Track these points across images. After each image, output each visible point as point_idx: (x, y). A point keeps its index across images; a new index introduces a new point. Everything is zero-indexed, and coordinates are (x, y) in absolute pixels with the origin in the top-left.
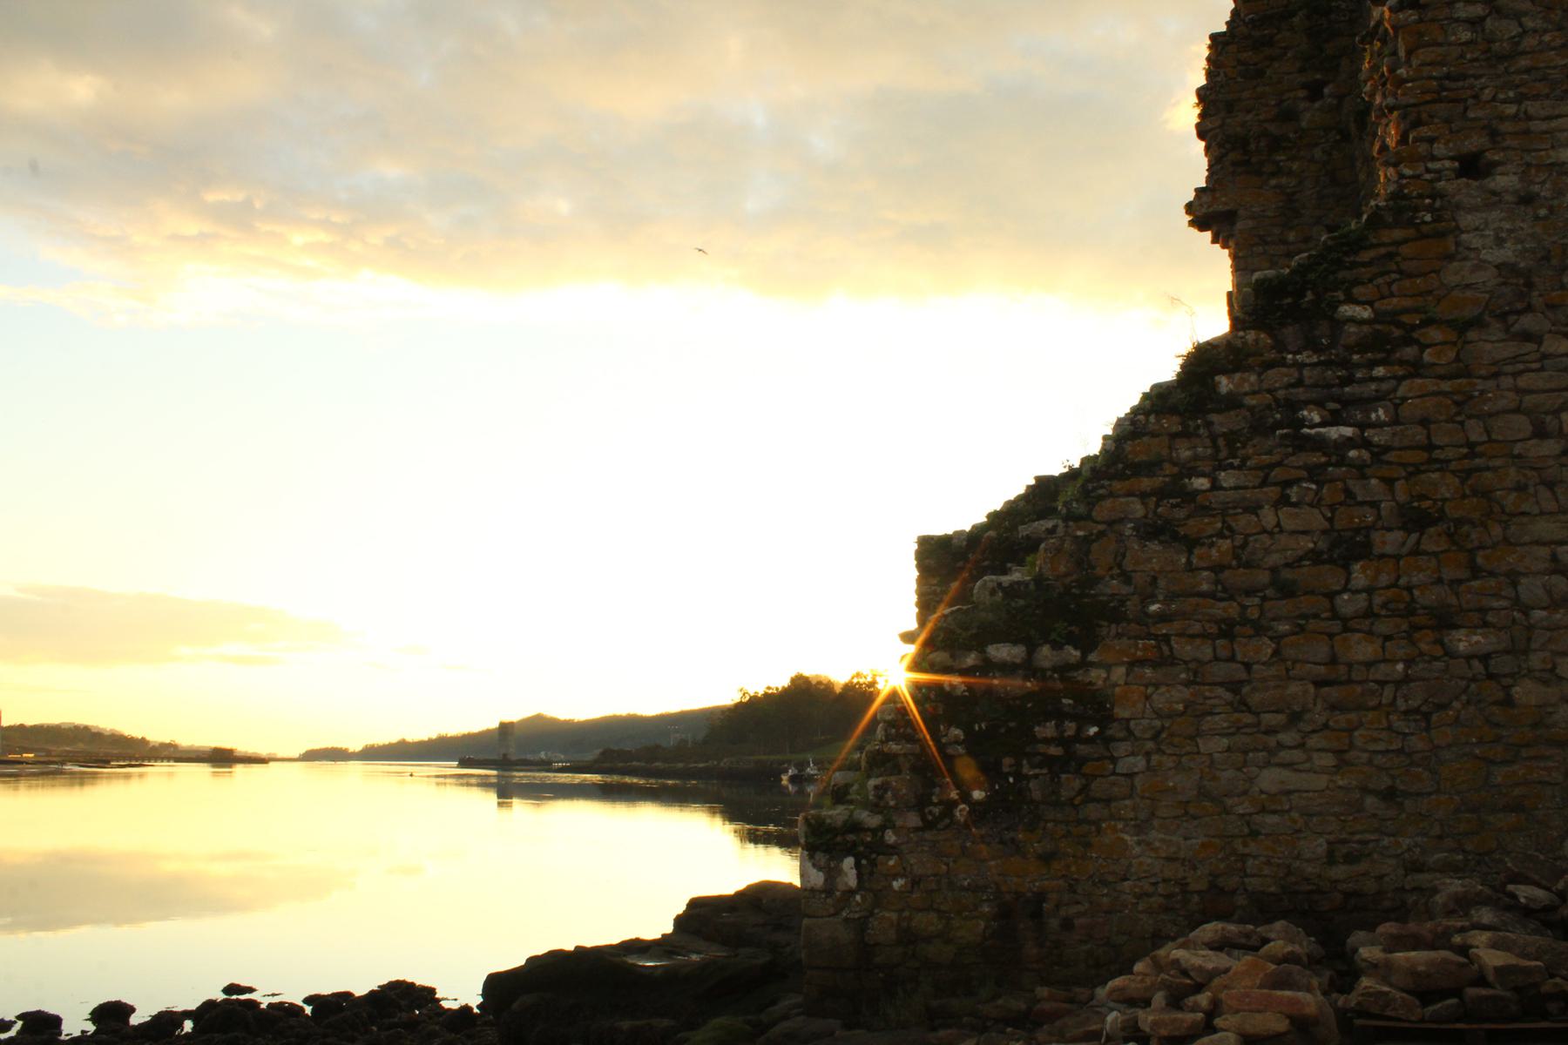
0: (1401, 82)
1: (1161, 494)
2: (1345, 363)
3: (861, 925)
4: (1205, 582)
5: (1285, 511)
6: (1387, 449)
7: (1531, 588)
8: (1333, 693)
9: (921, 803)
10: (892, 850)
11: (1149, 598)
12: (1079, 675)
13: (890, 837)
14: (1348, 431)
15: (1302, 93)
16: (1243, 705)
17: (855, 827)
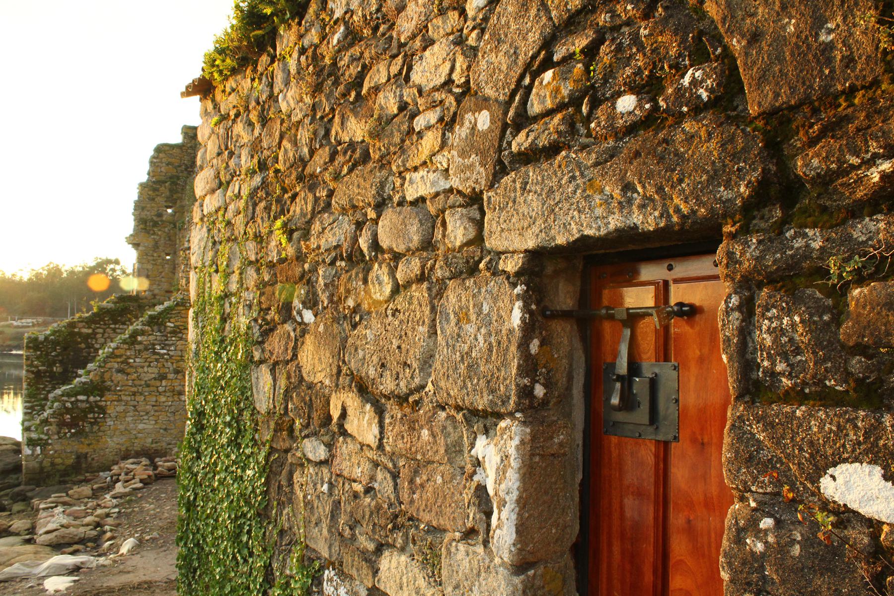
1: (122, 362)
2: (166, 336)
3: (41, 462)
4: (130, 383)
8: (156, 408)
9: (59, 433)
10: (50, 444)
11: (117, 386)
12: (100, 403)
13: (50, 441)
16: (136, 410)
17: (41, 439)
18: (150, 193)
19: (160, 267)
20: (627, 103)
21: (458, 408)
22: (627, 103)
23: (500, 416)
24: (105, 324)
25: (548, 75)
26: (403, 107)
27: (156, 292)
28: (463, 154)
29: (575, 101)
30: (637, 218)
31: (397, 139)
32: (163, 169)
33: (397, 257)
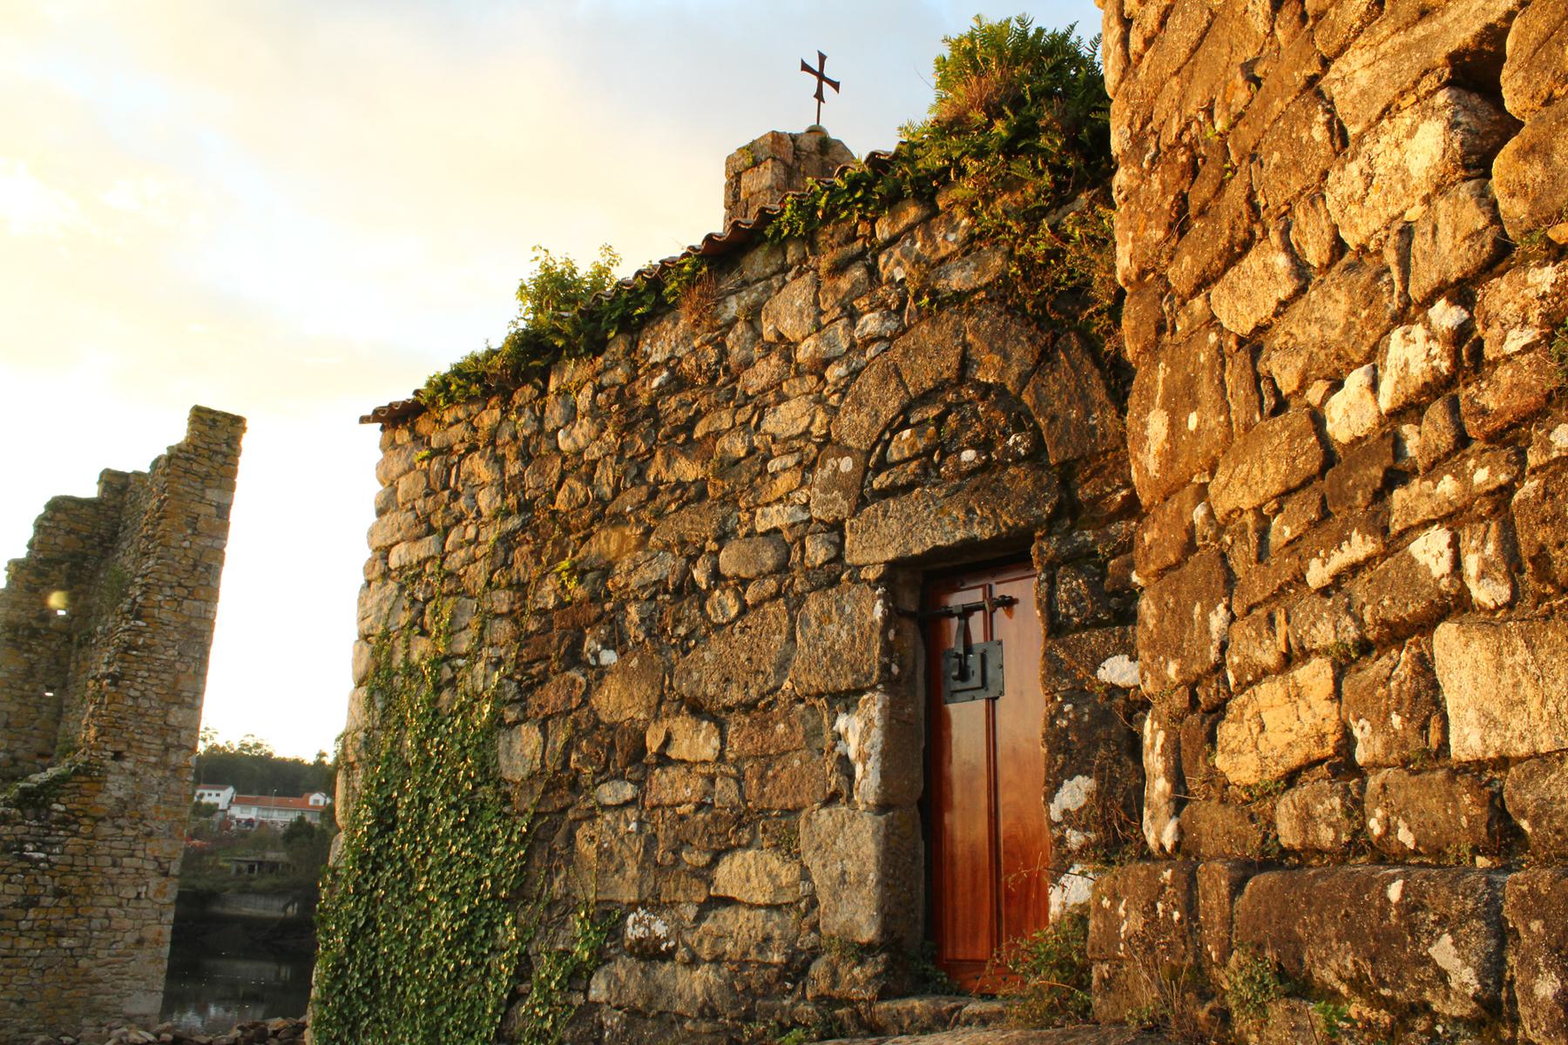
0: (102, 715)
2: (49, 828)
5: (8, 885)
6: (56, 864)
7: (95, 923)
14: (42, 855)
18: (31, 578)
19: (32, 710)
20: (968, 455)
21: (819, 695)
22: (968, 455)
23: (861, 692)
25: (907, 433)
26: (752, 451)
27: (20, 753)
28: (824, 490)
29: (928, 453)
30: (977, 531)
31: (745, 478)
32: (59, 540)
33: (745, 582)
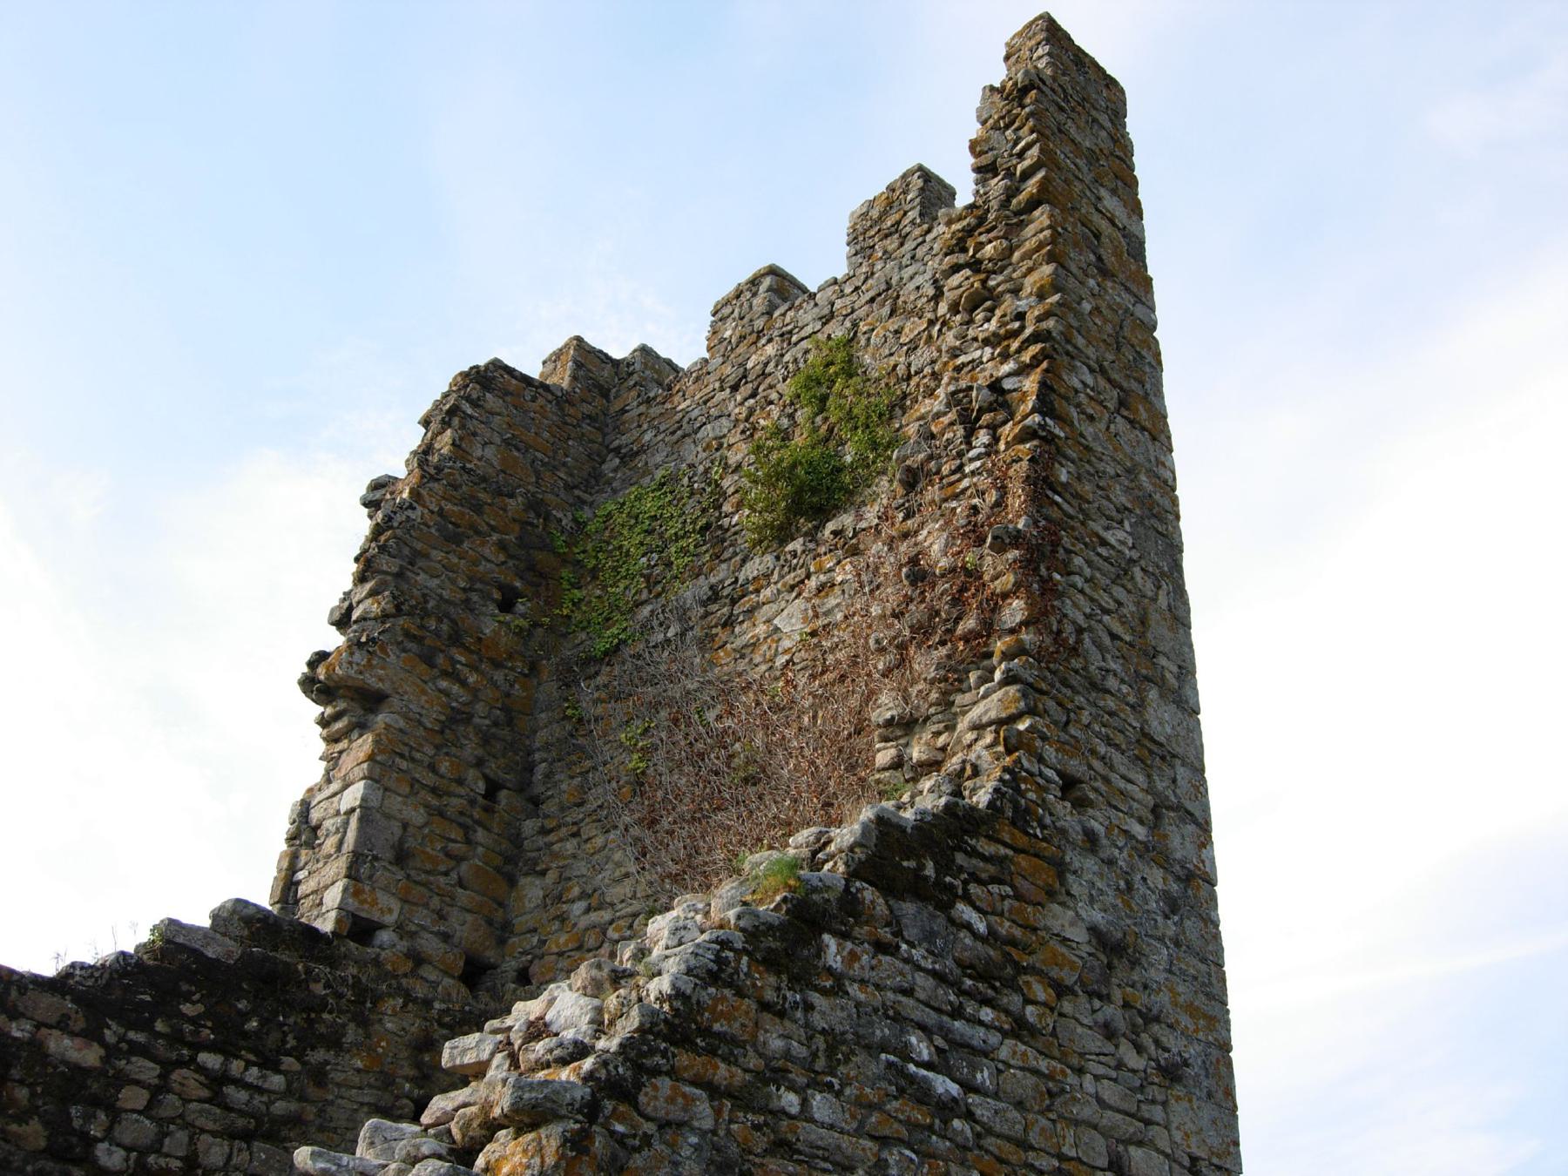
15: (497, 595)
24: (175, 1038)
